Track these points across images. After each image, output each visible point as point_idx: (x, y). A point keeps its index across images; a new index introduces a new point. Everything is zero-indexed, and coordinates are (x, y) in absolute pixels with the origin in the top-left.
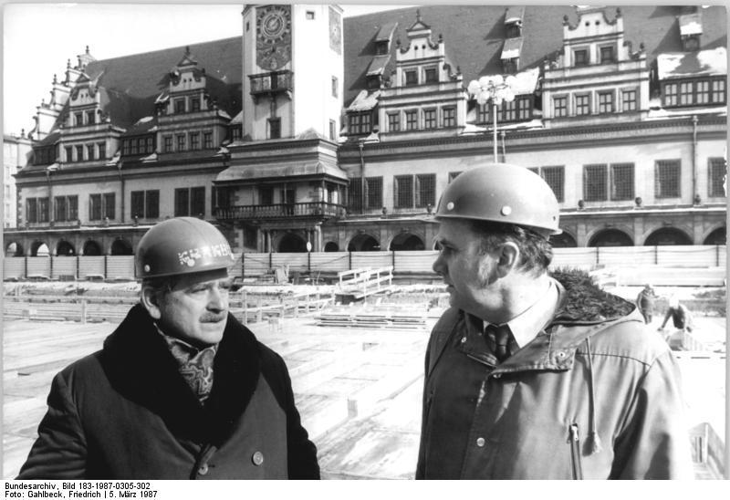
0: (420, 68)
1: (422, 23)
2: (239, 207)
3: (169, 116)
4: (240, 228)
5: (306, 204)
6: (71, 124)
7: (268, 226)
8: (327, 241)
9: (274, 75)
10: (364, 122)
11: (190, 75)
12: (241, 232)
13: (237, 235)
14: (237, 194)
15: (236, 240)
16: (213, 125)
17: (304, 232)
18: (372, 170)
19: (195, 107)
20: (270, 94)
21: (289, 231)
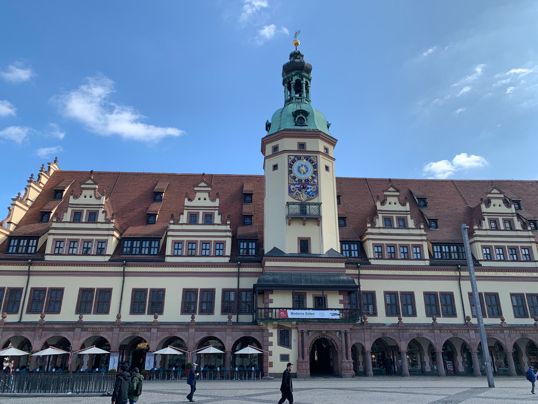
0: (394, 216)
1: (395, 188)
2: (272, 309)
3: (182, 224)
4: (274, 328)
6: (84, 220)
8: (354, 342)
10: (352, 249)
11: (206, 195)
12: (275, 332)
13: (271, 334)
14: (271, 297)
15: (270, 339)
16: (226, 237)
17: (338, 333)
18: (365, 286)
19: (209, 219)
21: (324, 332)
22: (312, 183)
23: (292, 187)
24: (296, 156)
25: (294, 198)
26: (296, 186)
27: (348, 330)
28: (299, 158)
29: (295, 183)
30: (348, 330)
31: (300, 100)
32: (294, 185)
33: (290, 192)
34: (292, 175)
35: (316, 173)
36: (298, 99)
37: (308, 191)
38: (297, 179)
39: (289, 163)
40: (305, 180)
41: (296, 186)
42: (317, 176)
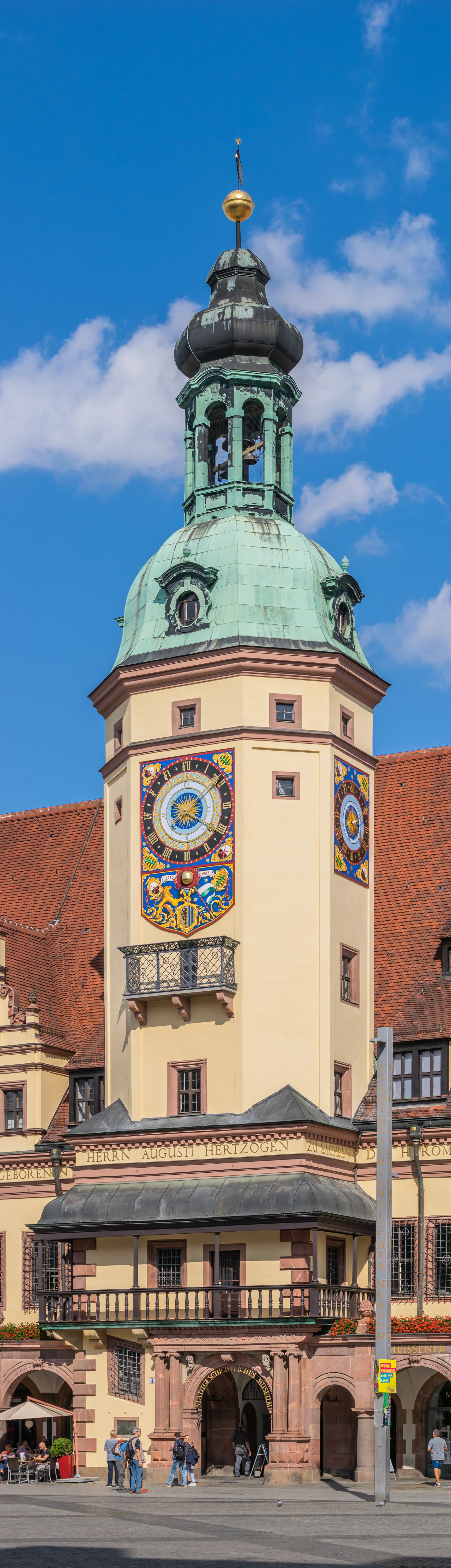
5: (270, 1288)
7: (172, 1345)
9: (189, 947)
20: (176, 1000)
22: (215, 858)
23: (153, 884)
24: (163, 762)
25: (158, 925)
26: (165, 879)
27: (293, 1349)
28: (174, 767)
29: (161, 866)
30: (293, 1349)
31: (220, 501)
32: (157, 874)
33: (147, 903)
34: (152, 840)
35: (227, 817)
36: (214, 495)
37: (203, 890)
38: (167, 854)
39: (142, 793)
40: (193, 852)
41: (165, 879)
42: (232, 829)
